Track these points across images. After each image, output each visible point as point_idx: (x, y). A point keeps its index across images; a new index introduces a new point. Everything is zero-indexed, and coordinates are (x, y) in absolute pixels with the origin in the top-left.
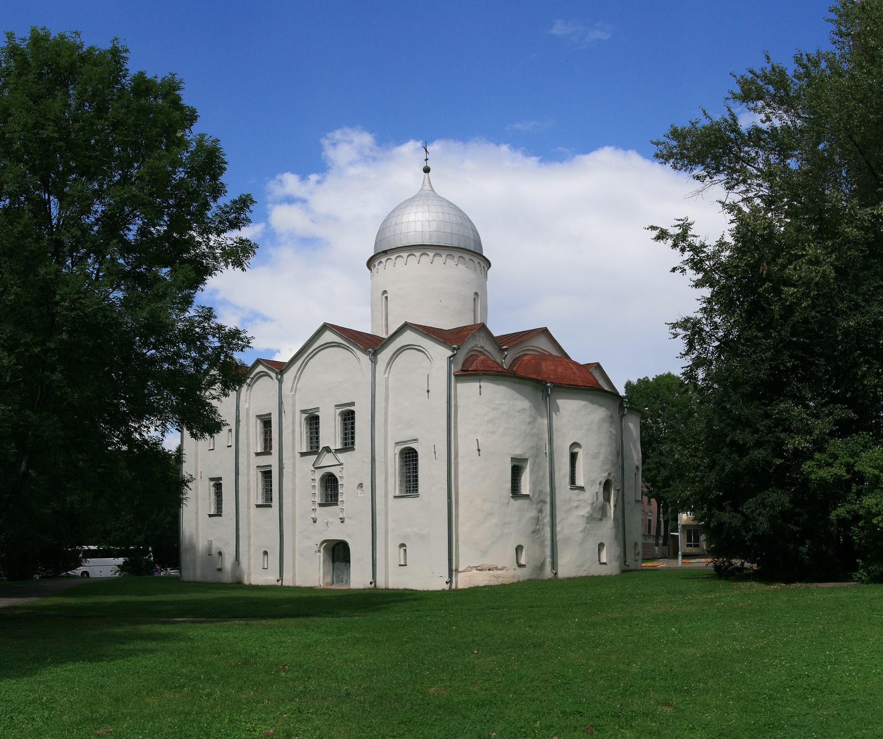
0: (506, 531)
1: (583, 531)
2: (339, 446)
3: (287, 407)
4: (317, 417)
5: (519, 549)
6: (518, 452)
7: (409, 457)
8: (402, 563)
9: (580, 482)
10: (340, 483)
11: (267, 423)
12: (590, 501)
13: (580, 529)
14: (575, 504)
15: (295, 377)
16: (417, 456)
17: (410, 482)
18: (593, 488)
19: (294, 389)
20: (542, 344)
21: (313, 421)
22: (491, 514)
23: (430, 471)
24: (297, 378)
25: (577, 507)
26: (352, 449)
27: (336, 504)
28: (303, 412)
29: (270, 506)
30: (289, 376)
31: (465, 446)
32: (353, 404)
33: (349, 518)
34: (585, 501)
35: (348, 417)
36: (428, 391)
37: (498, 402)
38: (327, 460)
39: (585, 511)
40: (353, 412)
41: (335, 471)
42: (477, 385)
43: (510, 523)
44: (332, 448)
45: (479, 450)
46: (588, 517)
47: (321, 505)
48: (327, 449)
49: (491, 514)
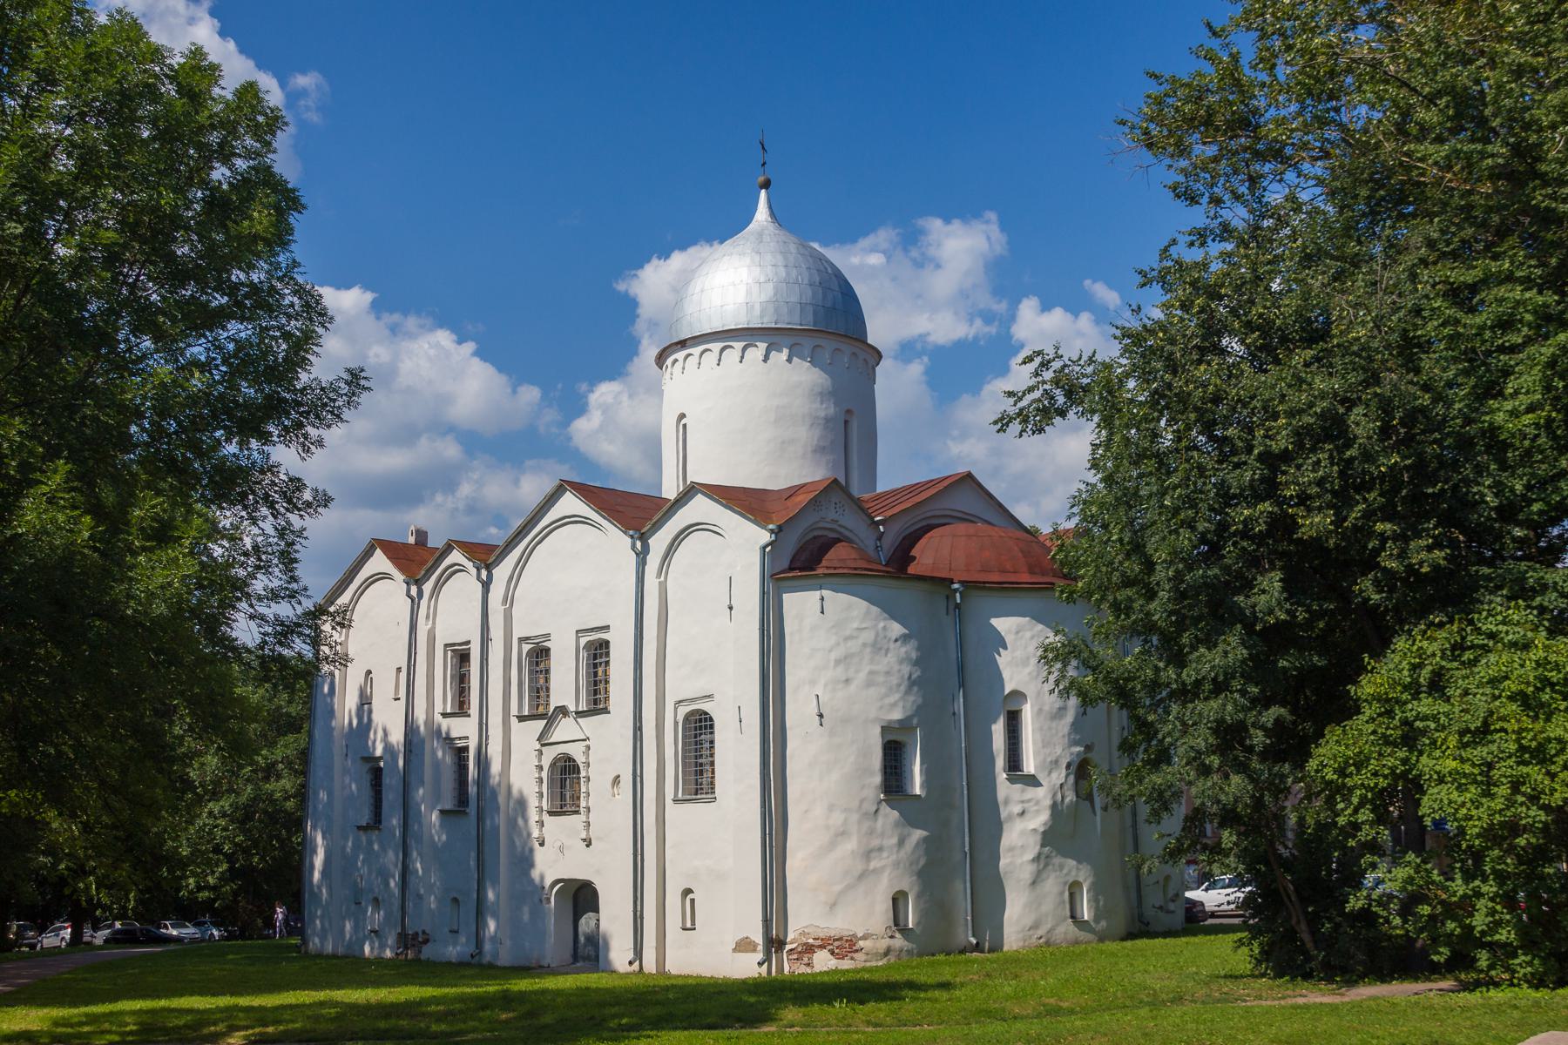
0: (874, 864)
1: (1037, 859)
2: (583, 707)
3: (497, 632)
4: (545, 652)
5: (898, 900)
6: (897, 715)
7: (699, 726)
8: (689, 925)
9: (1029, 765)
10: (583, 774)
11: (463, 658)
12: (1048, 802)
13: (1030, 855)
14: (1017, 809)
15: (511, 578)
16: (712, 726)
17: (699, 778)
18: (1054, 775)
19: (509, 600)
20: (963, 502)
21: (540, 654)
22: (843, 833)
23: (735, 754)
24: (514, 579)
25: (1023, 813)
26: (606, 711)
27: (577, 812)
28: (521, 640)
29: (464, 813)
30: (502, 572)
31: (799, 710)
32: (607, 627)
33: (599, 839)
34: (1037, 803)
35: (598, 652)
36: (731, 608)
37: (855, 625)
38: (565, 729)
39: (1039, 820)
40: (607, 643)
41: (576, 752)
42: (817, 594)
43: (880, 849)
44: (572, 708)
45: (821, 716)
46: (1044, 833)
47: (551, 813)
48: (562, 710)
49: (843, 833)
